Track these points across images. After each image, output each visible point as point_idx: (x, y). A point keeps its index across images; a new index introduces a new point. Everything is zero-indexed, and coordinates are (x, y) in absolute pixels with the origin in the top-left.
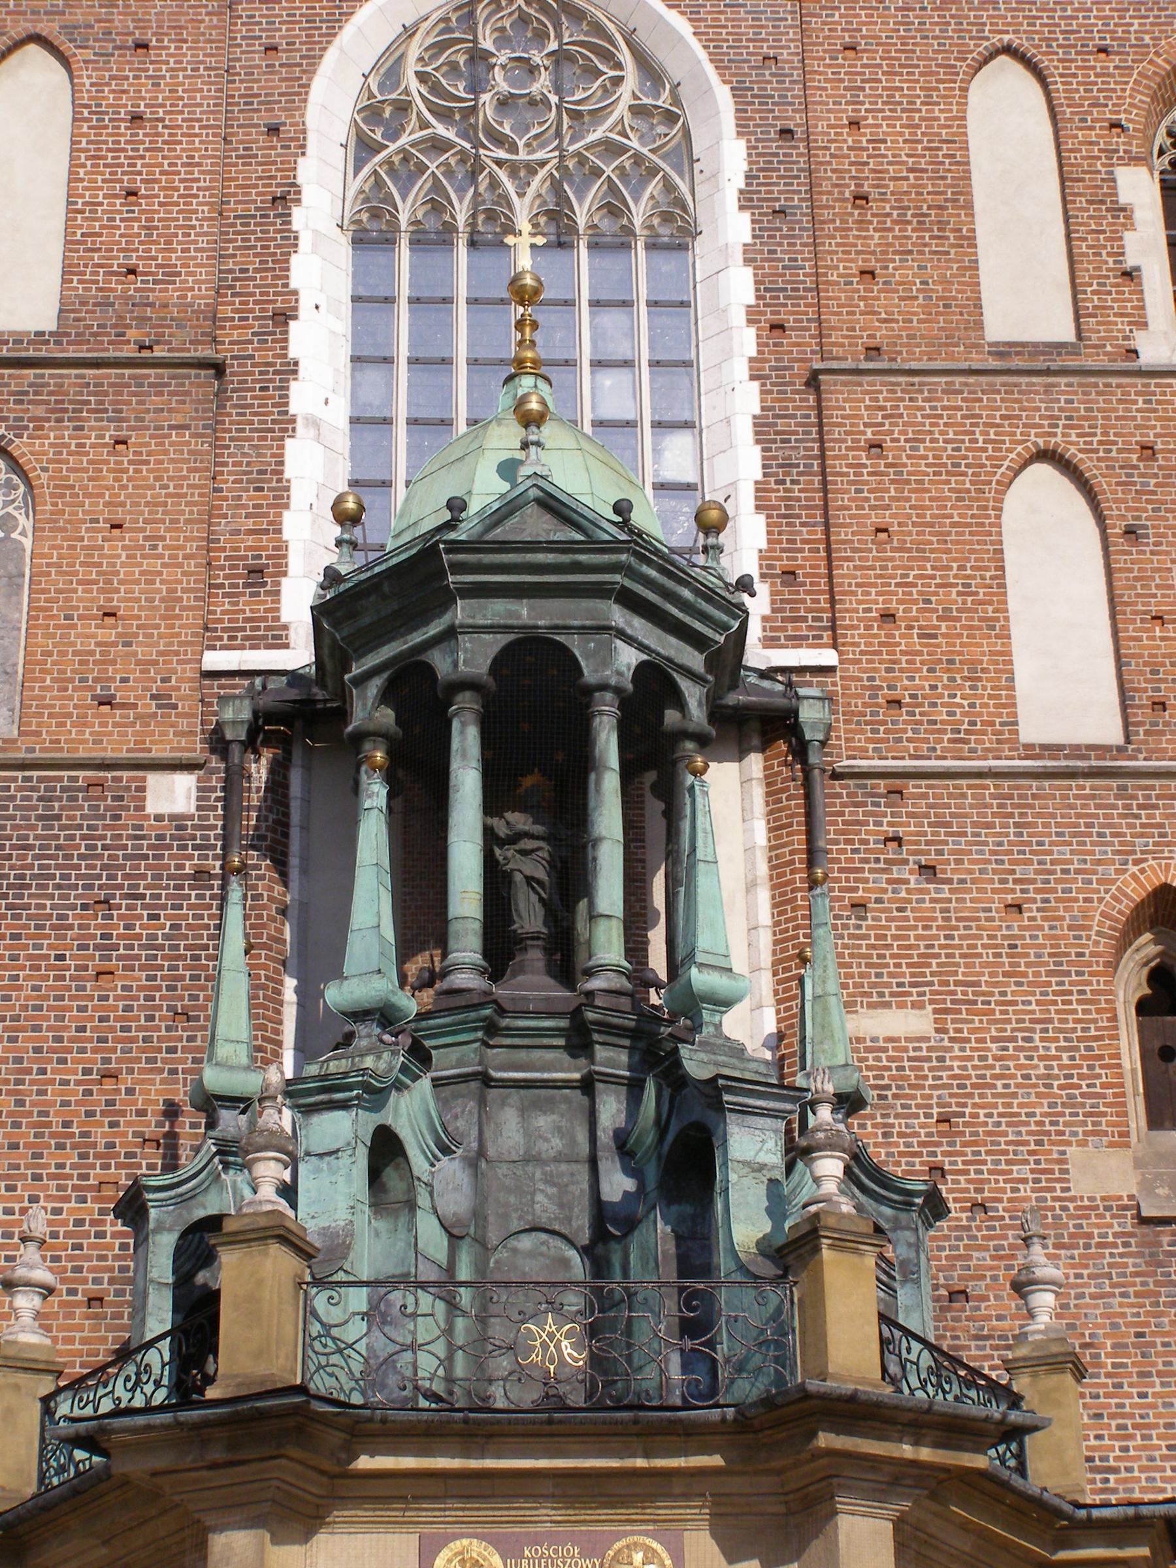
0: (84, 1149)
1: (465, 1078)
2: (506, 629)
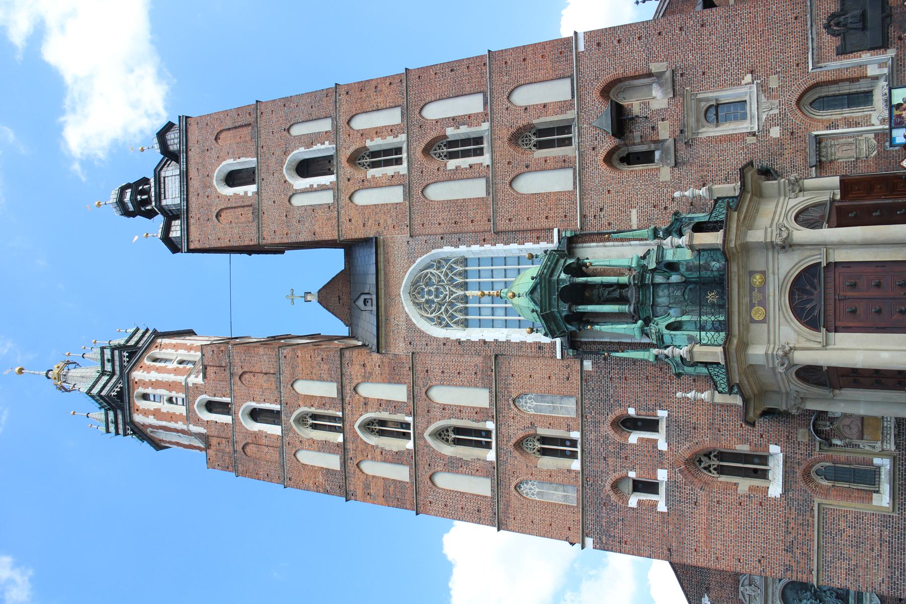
0: (662, 383)
1: (652, 309)
2: (558, 301)
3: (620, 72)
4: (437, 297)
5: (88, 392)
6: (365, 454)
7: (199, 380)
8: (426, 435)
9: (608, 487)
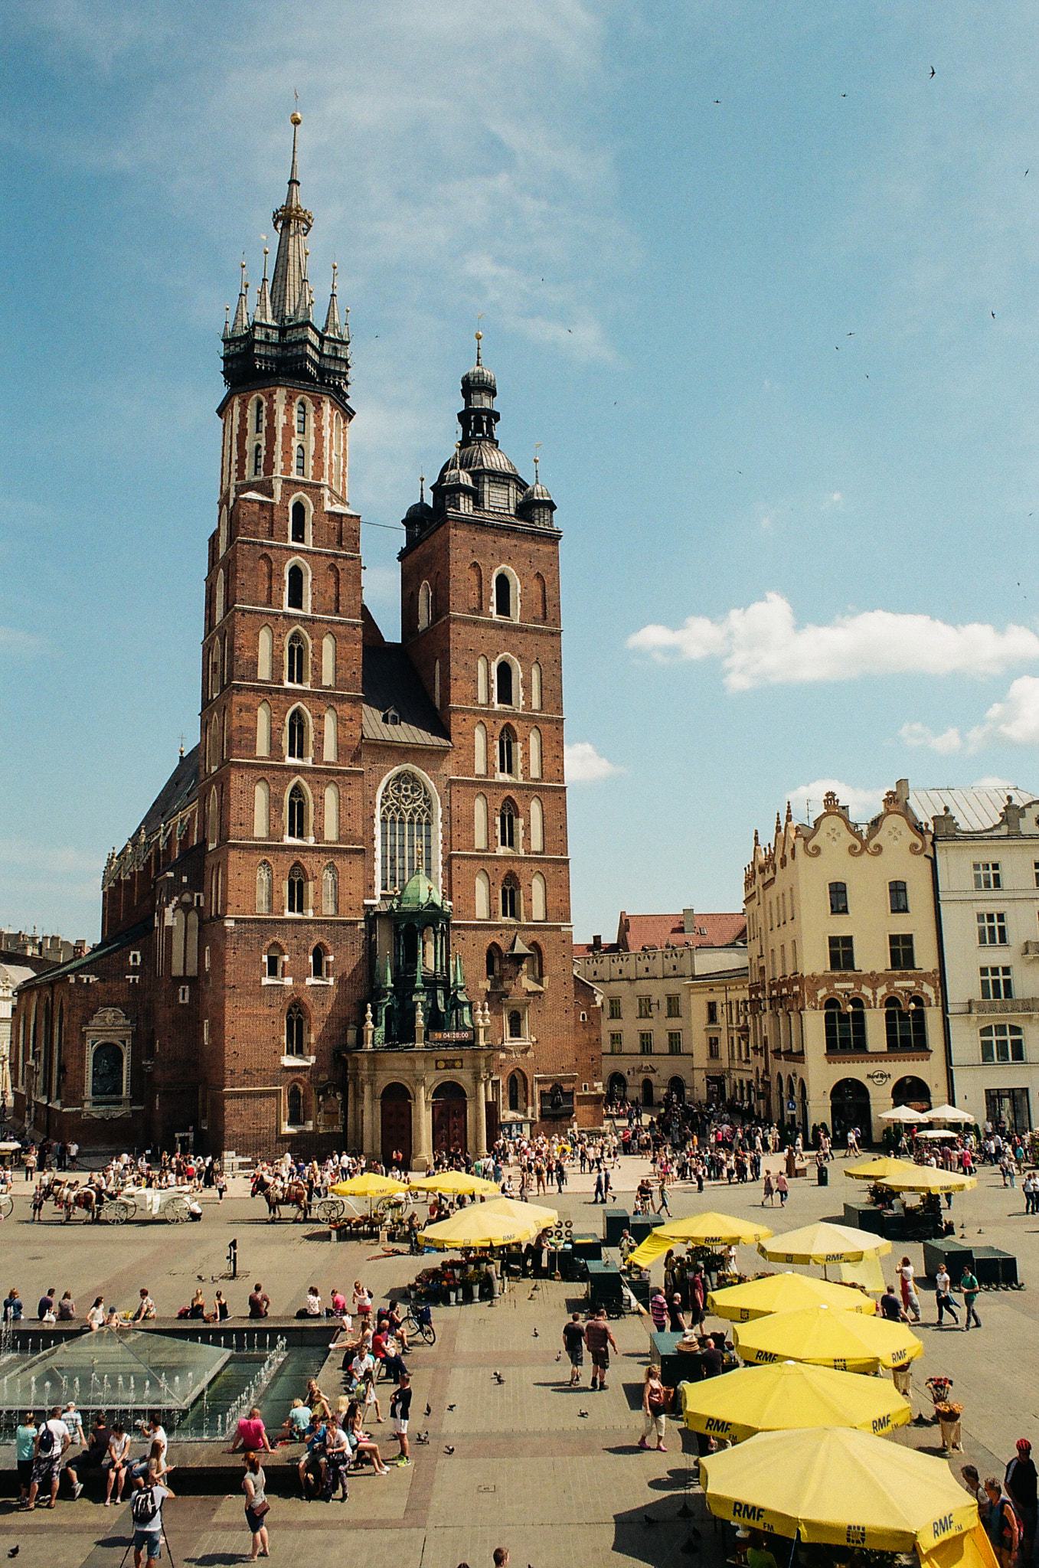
3: (545, 956)
4: (404, 796)
5: (308, 324)
6: (276, 711)
7: (328, 507)
8: (298, 778)
9: (275, 939)
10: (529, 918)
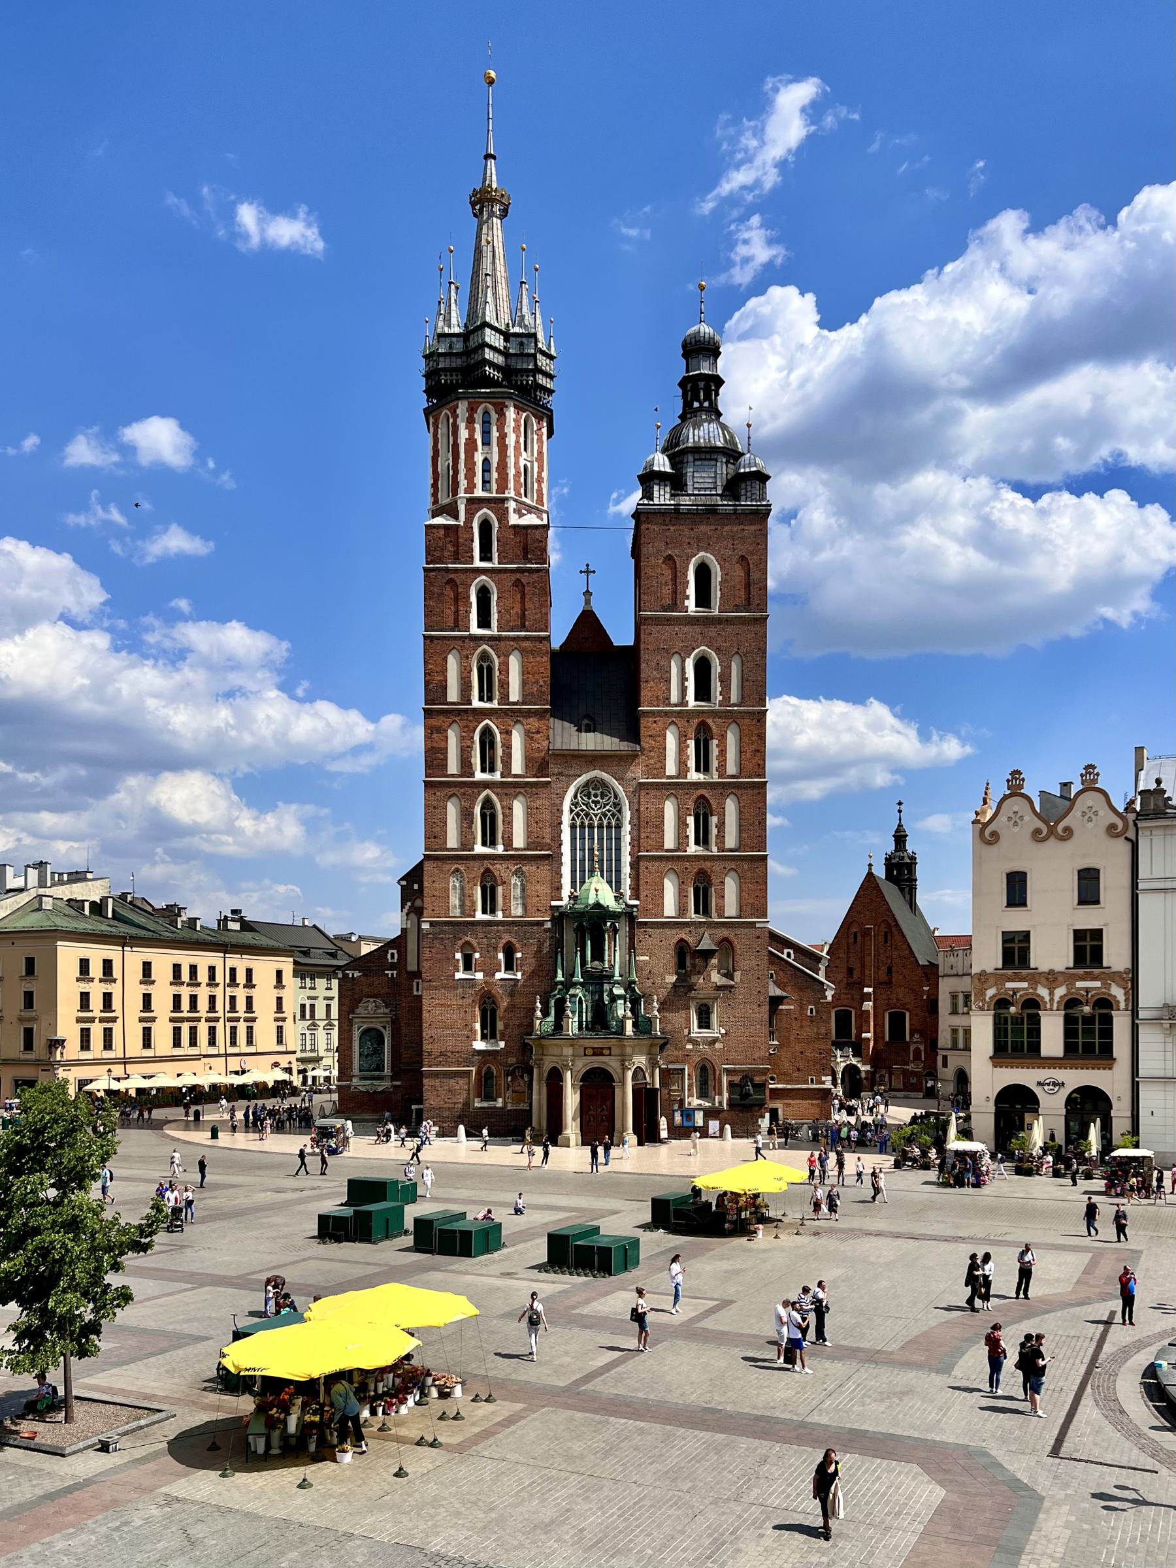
7: (514, 519)
8: (488, 791)
9: (467, 939)
10: (721, 912)
